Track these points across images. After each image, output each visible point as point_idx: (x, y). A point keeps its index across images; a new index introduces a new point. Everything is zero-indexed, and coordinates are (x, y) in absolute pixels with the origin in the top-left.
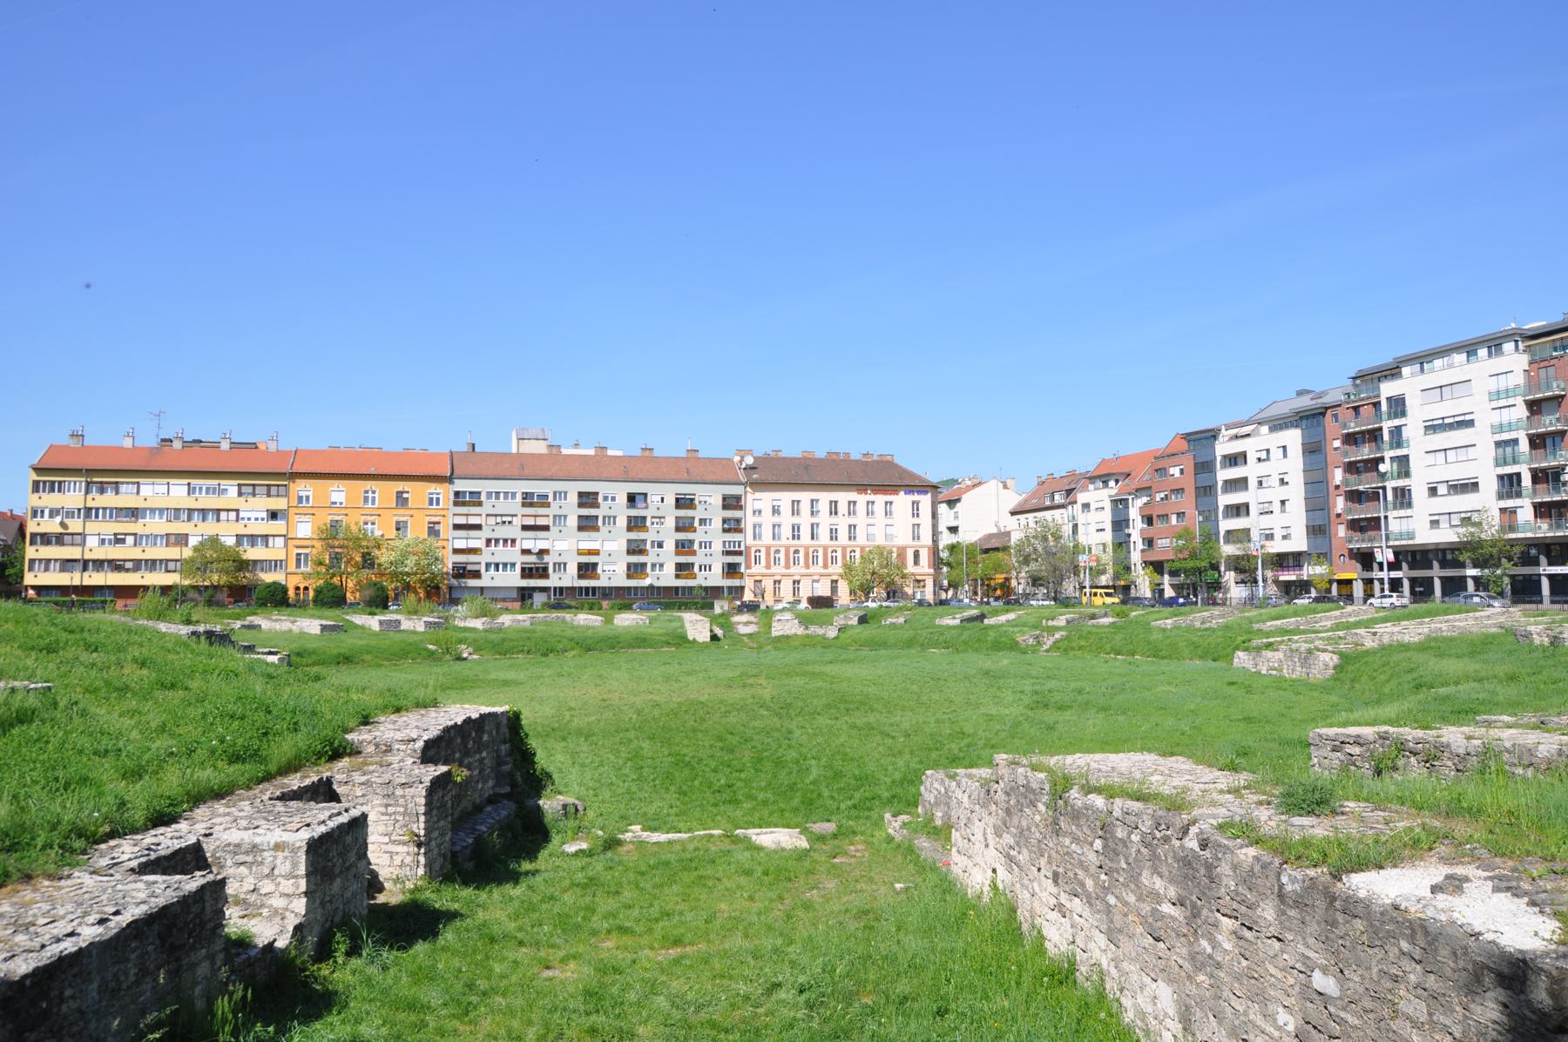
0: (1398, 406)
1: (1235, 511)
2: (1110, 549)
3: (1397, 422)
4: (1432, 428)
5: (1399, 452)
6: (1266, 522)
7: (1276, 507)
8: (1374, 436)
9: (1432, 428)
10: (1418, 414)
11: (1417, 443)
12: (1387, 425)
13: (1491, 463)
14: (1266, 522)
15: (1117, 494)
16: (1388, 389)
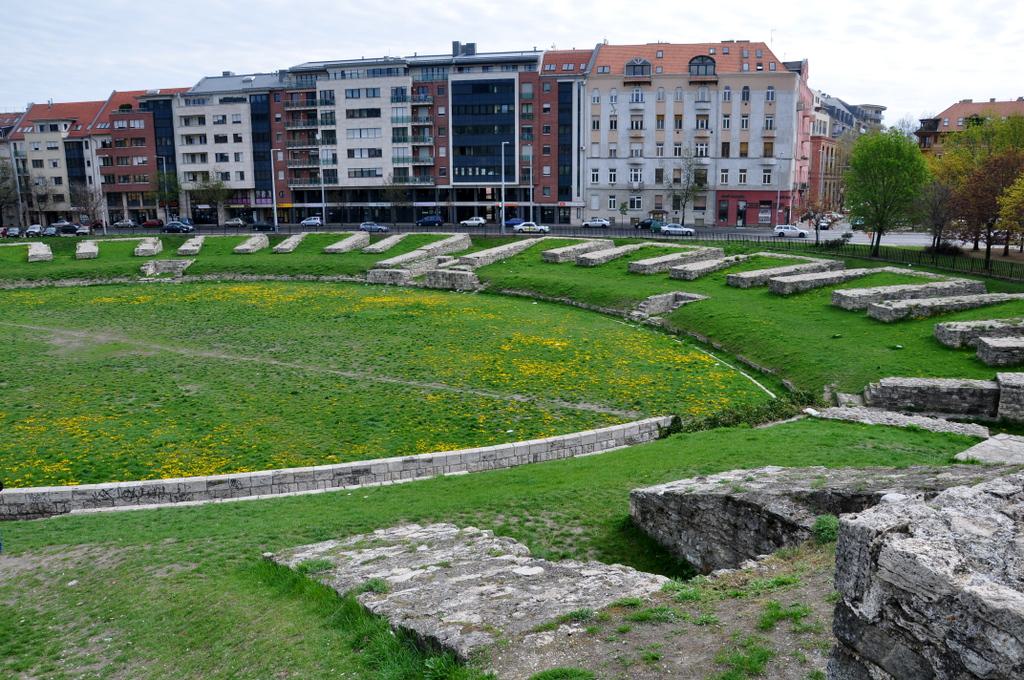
0: (329, 99)
1: (190, 158)
2: (65, 180)
3: (328, 108)
4: (351, 114)
5: (328, 128)
6: (223, 167)
7: (232, 158)
8: (312, 115)
9: (351, 114)
10: (342, 105)
11: (342, 126)
12: (321, 110)
13: (390, 140)
14: (223, 167)
15: (68, 138)
16: (322, 85)
